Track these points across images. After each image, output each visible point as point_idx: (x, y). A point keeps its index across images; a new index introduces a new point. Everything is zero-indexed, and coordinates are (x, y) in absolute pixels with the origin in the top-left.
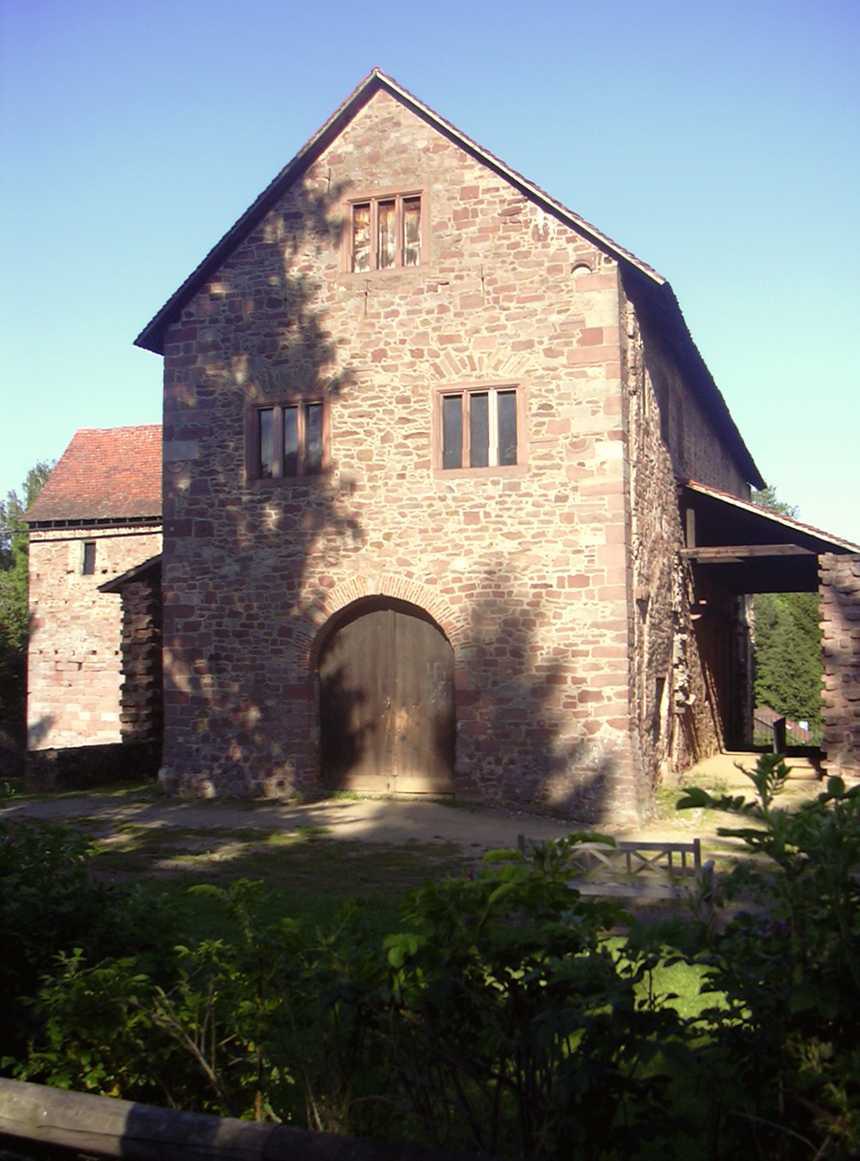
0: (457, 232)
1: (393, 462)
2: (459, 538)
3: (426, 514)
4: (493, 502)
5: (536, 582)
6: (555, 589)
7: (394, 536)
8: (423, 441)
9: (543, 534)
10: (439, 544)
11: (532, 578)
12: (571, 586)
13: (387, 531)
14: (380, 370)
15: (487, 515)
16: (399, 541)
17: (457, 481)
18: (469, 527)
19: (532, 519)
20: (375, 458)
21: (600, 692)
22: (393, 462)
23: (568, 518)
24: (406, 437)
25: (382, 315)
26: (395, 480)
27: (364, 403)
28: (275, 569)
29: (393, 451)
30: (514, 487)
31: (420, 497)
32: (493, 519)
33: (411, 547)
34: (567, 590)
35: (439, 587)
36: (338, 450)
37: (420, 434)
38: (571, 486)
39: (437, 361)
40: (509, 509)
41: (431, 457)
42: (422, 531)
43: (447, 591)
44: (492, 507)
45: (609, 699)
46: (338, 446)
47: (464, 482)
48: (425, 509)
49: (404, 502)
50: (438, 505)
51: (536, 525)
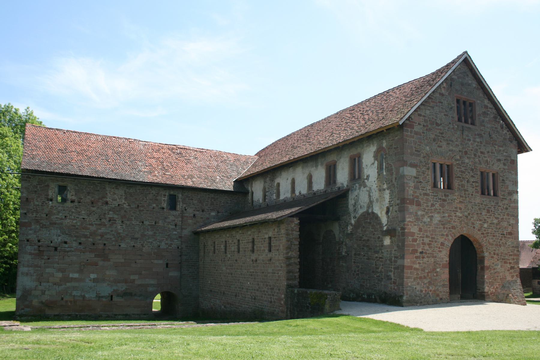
0: (483, 119)
1: (471, 190)
2: (485, 217)
3: (478, 208)
4: (492, 207)
5: (502, 233)
6: (505, 235)
7: (471, 214)
8: (477, 184)
9: (503, 219)
10: (481, 218)
11: (501, 232)
12: (509, 235)
13: (468, 212)
14: (466, 157)
15: (492, 211)
16: (472, 216)
17: (485, 199)
18: (488, 214)
19: (501, 214)
20: (466, 187)
21: (514, 266)
22: (471, 190)
23: (508, 215)
24: (473, 182)
25: (467, 139)
26: (470, 196)
27: (462, 168)
28: (440, 221)
29: (470, 186)
30: (497, 203)
31: (477, 202)
32: (493, 212)
33: (475, 218)
34: (508, 236)
35: (481, 232)
36: (456, 182)
37: (476, 182)
38: (509, 205)
39: (480, 159)
40: (496, 210)
41: (479, 190)
42: (477, 214)
43: (483, 234)
44: (493, 209)
45: (516, 268)
46: (456, 181)
47: (486, 200)
48: (478, 206)
49: (473, 204)
50: (481, 206)
51: (502, 216)
